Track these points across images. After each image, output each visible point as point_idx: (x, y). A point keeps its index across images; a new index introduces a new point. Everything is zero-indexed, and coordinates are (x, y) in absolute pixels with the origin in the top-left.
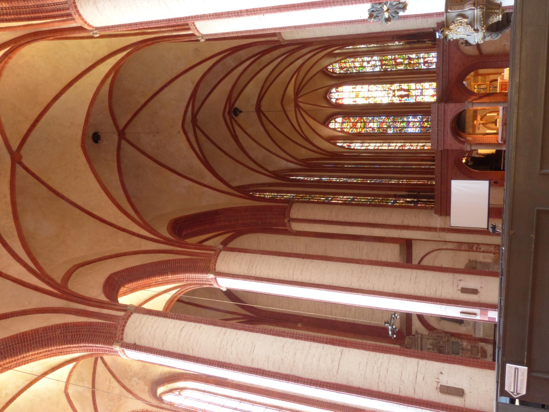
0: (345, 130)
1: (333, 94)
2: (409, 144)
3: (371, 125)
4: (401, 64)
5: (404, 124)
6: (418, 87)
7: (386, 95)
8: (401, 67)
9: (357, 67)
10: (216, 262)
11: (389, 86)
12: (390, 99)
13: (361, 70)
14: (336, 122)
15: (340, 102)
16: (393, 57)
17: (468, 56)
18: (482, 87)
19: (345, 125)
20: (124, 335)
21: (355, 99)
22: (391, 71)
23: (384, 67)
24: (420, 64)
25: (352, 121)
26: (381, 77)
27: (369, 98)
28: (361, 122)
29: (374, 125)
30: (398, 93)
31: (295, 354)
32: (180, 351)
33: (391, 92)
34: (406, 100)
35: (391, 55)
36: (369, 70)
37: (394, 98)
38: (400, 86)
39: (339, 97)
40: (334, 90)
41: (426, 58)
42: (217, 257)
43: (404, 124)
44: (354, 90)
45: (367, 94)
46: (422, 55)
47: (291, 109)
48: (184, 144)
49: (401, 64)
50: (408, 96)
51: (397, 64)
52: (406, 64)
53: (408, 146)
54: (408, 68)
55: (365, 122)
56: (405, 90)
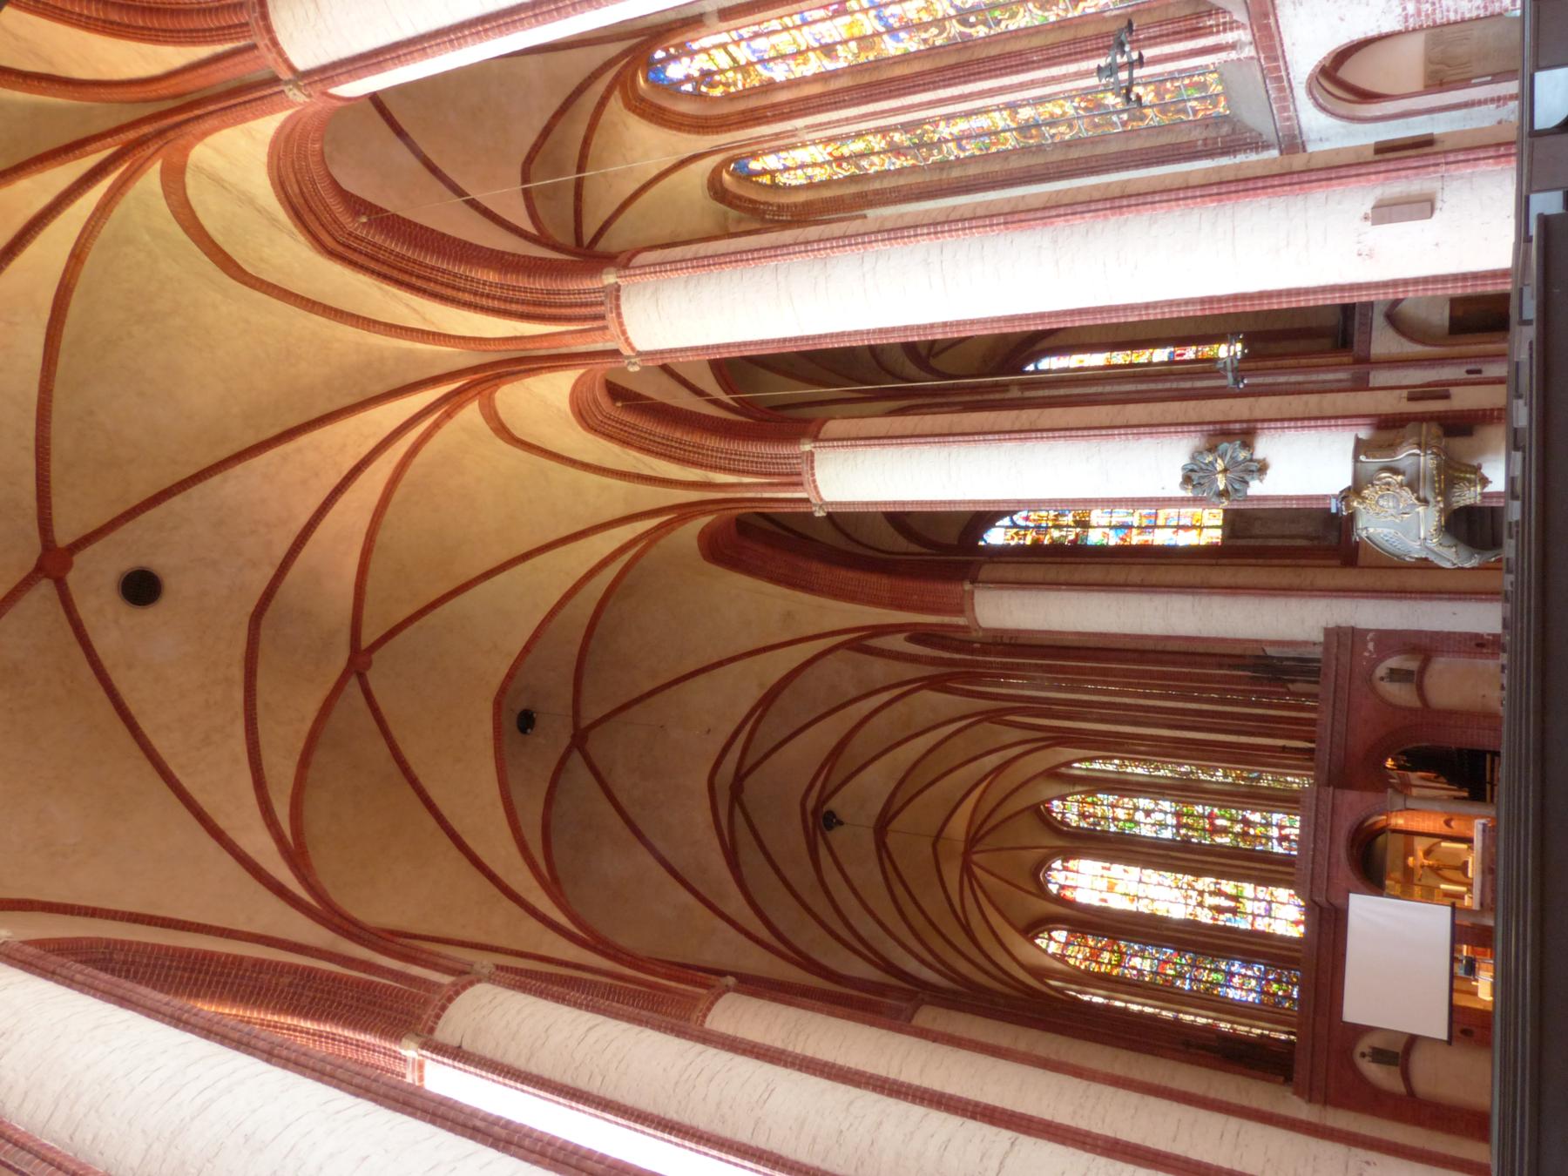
0: (1072, 961)
1: (1054, 873)
3: (1136, 962)
4: (1225, 831)
5: (1219, 977)
6: (1261, 896)
8: (1225, 840)
10: (709, 1009)
11: (1191, 878)
12: (1190, 910)
13: (1130, 829)
14: (1050, 938)
15: (1068, 894)
16: (1208, 810)
17: (1396, 708)
19: (1070, 951)
20: (441, 1023)
21: (1105, 895)
23: (1183, 831)
24: (1269, 838)
25: (1091, 943)
28: (1113, 952)
29: (1141, 964)
30: (1210, 900)
31: (881, 1123)
32: (568, 1080)
35: (1204, 805)
36: (1146, 831)
39: (1068, 883)
40: (1057, 864)
42: (717, 999)
43: (1219, 977)
44: (1106, 873)
45: (1134, 889)
46: (1276, 818)
47: (952, 874)
48: (703, 816)
49: (1225, 831)
50: (1234, 911)
51: (1215, 830)
52: (1237, 835)
55: (1122, 954)
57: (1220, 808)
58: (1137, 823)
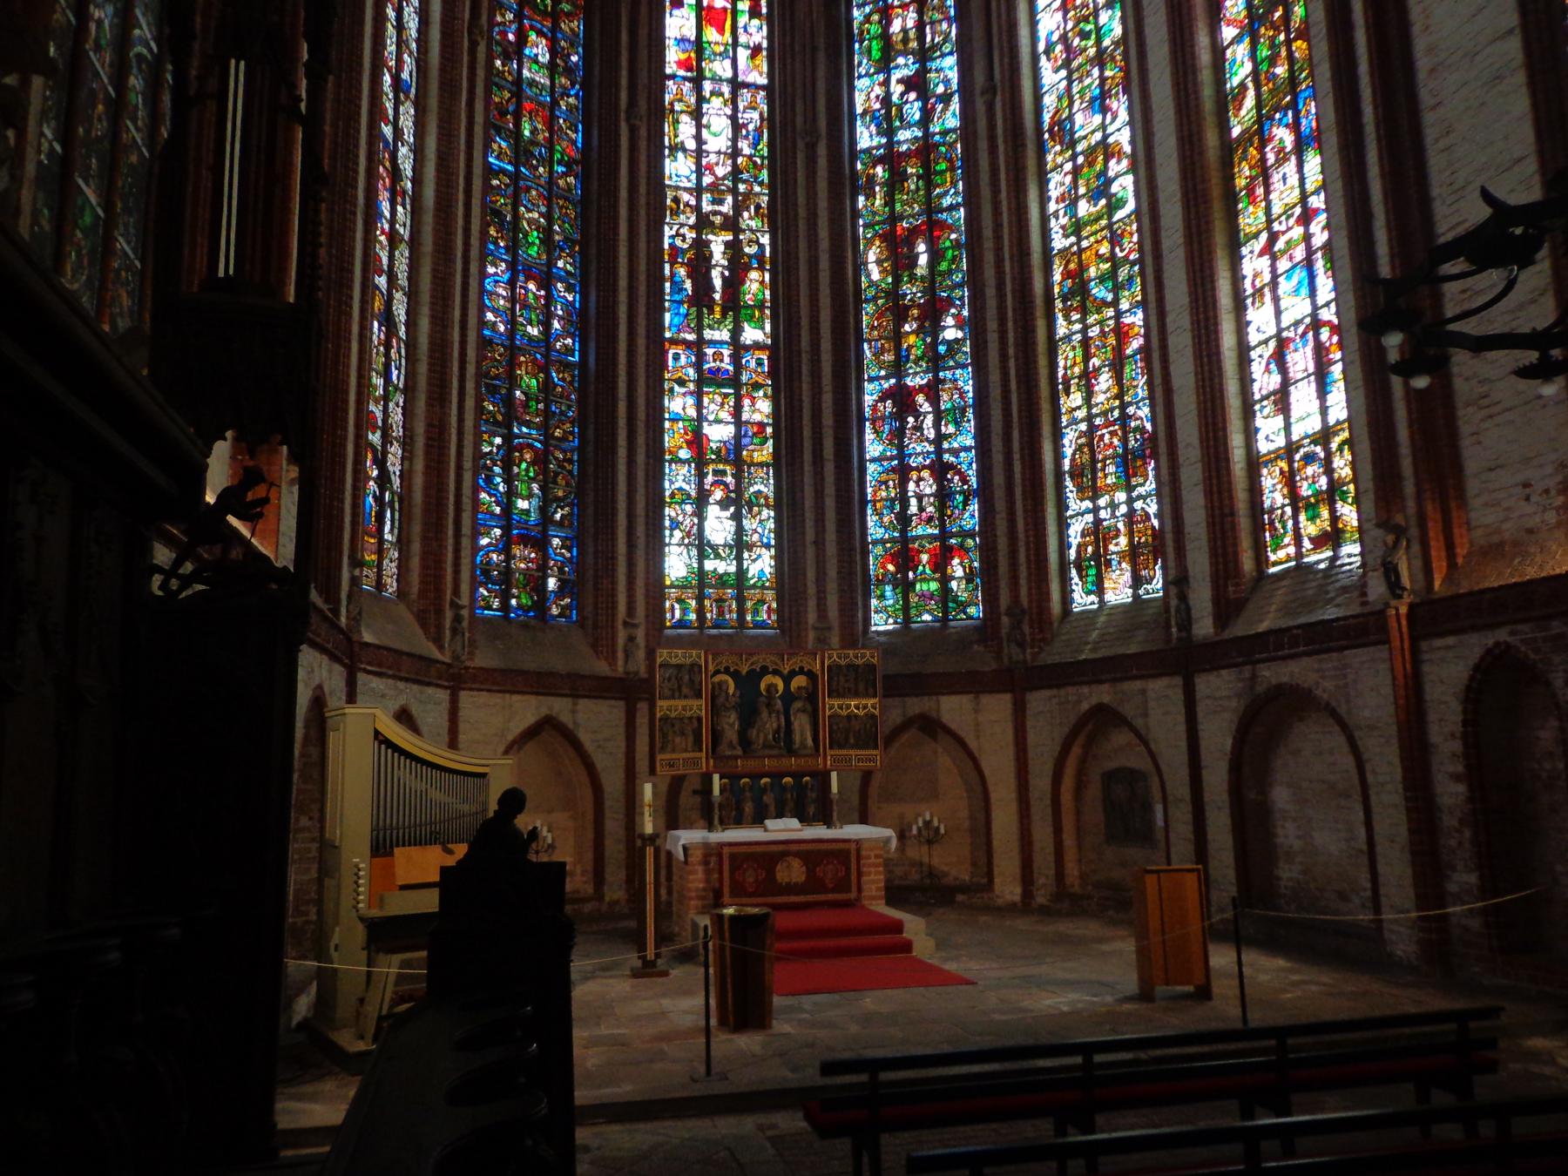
2: (404, 232)
3: (539, 49)
4: (900, 262)
6: (750, 360)
7: (707, 180)
9: (886, 20)
18: (801, 723)
22: (856, 214)
24: (898, 369)
26: (822, 150)
27: (697, 82)
30: (717, 246)
33: (726, 208)
34: (678, 287)
36: (866, 92)
37: (692, 221)
38: (760, 257)
41: (934, 399)
50: (702, 296)
52: (894, 294)
53: (393, 214)
54: (869, 308)
56: (734, 283)
57: (973, 243)
58: (885, 65)
